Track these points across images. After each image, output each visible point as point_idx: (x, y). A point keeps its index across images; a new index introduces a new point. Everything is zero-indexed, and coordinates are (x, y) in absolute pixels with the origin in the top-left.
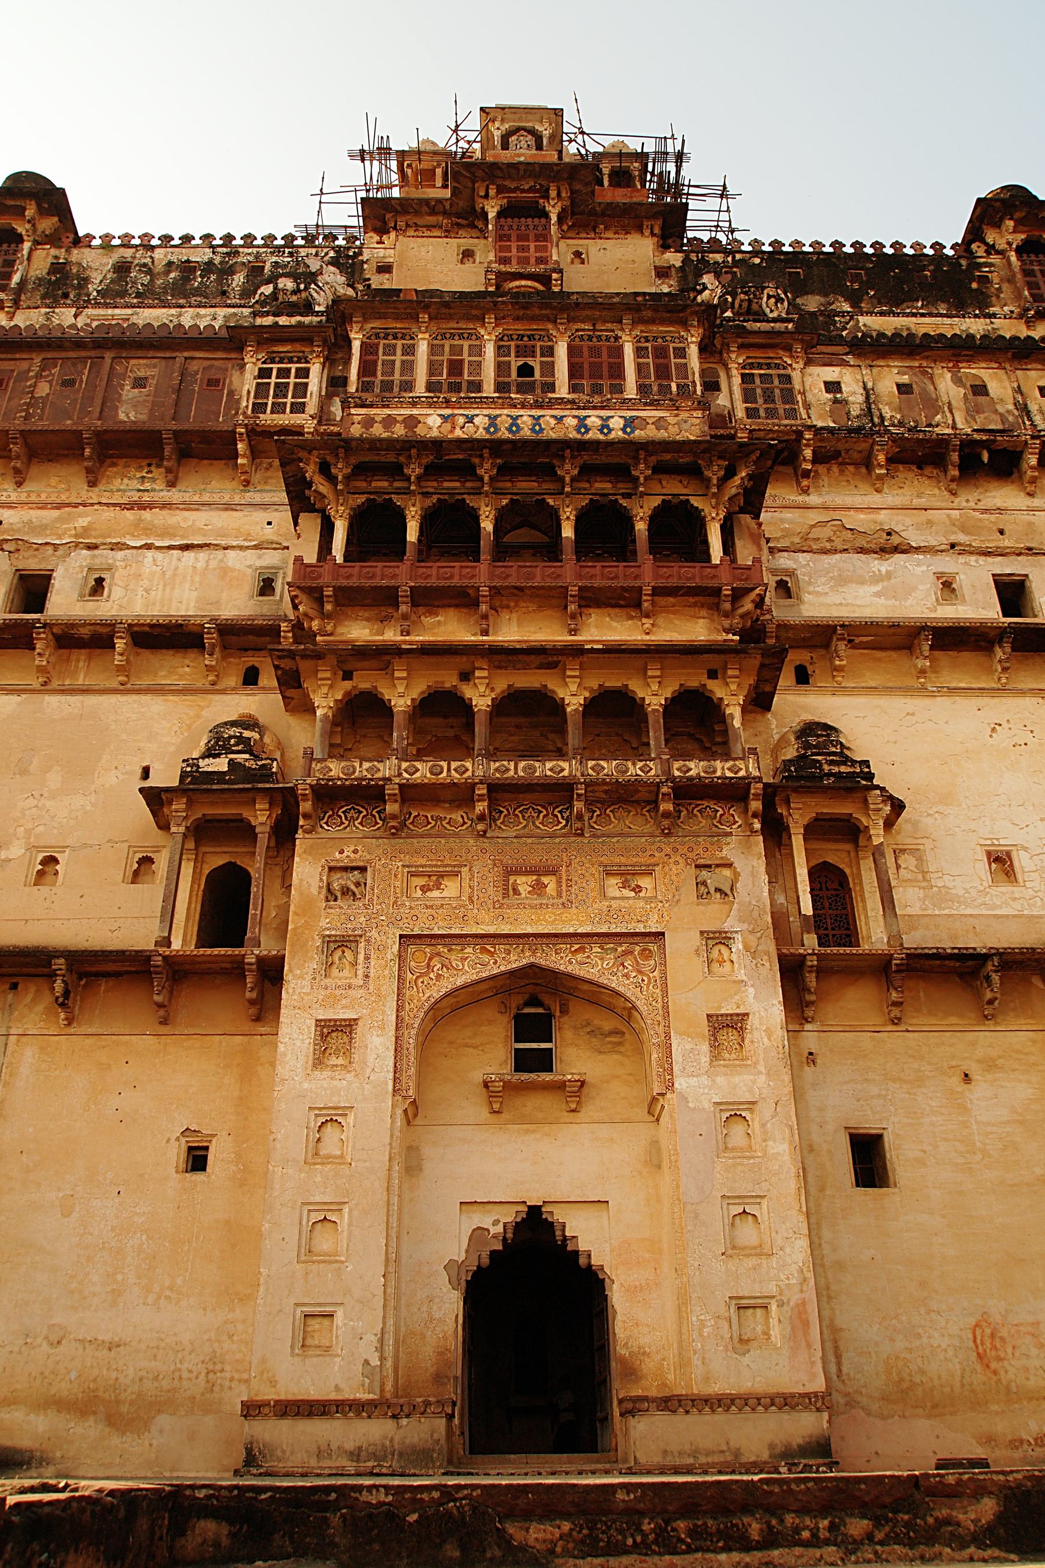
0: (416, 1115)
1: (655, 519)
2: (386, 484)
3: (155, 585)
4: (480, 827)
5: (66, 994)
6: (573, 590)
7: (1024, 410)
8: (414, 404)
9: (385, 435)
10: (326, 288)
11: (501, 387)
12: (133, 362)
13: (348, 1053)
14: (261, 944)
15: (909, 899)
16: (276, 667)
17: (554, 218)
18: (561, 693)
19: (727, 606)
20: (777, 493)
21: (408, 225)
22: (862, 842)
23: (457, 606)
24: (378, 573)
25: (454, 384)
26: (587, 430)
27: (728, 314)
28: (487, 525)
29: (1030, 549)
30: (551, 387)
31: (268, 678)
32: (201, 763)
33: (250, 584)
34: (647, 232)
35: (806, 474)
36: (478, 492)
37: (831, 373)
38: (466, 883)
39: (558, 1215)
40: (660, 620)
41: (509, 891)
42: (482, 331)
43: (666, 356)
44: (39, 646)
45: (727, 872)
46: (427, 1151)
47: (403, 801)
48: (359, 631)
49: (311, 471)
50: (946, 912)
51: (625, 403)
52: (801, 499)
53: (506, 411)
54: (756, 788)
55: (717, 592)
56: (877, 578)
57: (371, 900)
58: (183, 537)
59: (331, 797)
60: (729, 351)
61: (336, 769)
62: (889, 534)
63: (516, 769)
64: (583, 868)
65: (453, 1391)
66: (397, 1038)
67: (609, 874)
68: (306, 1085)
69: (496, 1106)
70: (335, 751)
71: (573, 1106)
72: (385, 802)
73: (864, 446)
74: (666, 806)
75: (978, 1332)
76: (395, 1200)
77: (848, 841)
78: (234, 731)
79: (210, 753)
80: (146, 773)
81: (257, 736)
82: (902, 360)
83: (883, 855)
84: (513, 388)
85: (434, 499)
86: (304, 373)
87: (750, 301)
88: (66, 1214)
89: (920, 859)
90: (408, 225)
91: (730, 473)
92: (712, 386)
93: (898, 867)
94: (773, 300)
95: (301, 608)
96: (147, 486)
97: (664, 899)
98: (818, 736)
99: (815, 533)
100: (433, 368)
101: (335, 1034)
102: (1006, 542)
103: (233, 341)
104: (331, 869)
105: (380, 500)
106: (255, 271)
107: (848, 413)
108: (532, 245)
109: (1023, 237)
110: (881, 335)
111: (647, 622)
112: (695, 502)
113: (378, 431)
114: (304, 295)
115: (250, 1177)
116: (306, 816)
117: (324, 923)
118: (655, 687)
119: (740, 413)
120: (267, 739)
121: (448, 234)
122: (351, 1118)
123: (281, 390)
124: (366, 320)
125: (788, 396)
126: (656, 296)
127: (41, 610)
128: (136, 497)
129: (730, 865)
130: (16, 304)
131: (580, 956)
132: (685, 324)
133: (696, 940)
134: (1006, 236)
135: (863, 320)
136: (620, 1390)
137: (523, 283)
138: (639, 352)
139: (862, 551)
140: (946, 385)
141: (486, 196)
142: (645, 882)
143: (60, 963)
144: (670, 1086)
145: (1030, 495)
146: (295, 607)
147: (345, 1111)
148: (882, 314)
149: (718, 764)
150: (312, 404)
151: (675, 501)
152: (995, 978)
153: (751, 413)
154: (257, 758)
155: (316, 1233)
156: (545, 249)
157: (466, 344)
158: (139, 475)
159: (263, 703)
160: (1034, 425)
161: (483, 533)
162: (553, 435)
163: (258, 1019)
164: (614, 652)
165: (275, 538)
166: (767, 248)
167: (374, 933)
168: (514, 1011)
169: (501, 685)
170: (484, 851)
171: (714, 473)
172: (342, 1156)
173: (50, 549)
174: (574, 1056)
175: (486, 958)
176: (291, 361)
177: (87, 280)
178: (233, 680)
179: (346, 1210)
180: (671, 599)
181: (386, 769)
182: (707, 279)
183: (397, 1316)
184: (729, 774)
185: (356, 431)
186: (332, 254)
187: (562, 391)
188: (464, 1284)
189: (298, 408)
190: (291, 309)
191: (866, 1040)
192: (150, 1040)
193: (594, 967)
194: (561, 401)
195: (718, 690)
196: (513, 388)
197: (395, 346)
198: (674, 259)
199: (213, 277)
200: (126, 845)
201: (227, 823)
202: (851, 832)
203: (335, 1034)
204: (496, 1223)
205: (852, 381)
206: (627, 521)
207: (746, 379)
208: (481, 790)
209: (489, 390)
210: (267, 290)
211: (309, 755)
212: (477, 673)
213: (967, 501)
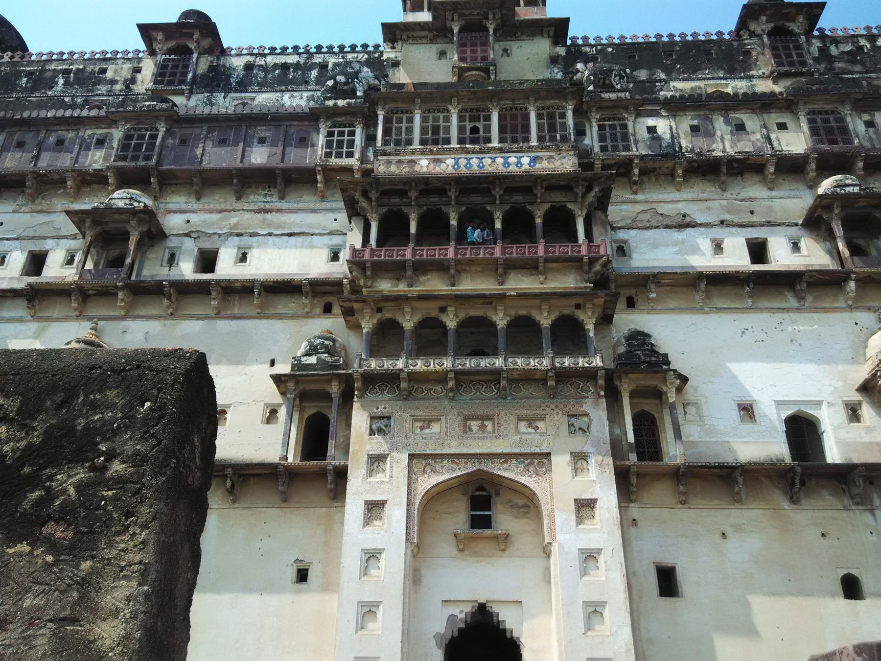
0: (418, 552)
1: (547, 217)
2: (398, 200)
3: (272, 261)
4: (451, 394)
5: (233, 486)
8: (413, 152)
9: (397, 172)
10: (363, 80)
12: (258, 128)
14: (333, 459)
15: (691, 431)
16: (341, 307)
17: (491, 31)
18: (494, 318)
19: (586, 268)
20: (619, 193)
23: (438, 270)
25: (435, 139)
26: (509, 165)
28: (454, 222)
29: (769, 222)
30: (488, 140)
32: (303, 359)
33: (325, 254)
34: (546, 35)
35: (635, 183)
36: (448, 204)
37: (651, 122)
38: (443, 426)
39: (495, 608)
40: (549, 276)
41: (467, 429)
42: (450, 108)
44: (214, 294)
45: (586, 419)
46: (424, 572)
47: (410, 381)
48: (385, 286)
49: (358, 196)
50: (713, 439)
51: (530, 149)
52: (632, 197)
53: (464, 156)
55: (580, 260)
56: (677, 243)
57: (393, 435)
58: (289, 229)
60: (591, 112)
61: (374, 364)
62: (684, 216)
63: (470, 363)
64: (507, 419)
66: (407, 510)
67: (520, 419)
68: (360, 537)
71: (503, 547)
73: (670, 164)
74: (551, 383)
76: (407, 600)
77: (656, 398)
78: (318, 341)
79: (308, 354)
81: (331, 344)
82: (694, 111)
83: (675, 408)
84: (468, 141)
85: (425, 208)
86: (352, 133)
87: (604, 79)
90: (408, 37)
91: (589, 189)
92: (580, 132)
93: (685, 413)
94: (617, 78)
95: (354, 273)
96: (268, 199)
97: (550, 433)
98: (638, 340)
100: (423, 131)
101: (374, 508)
102: (755, 219)
105: (395, 209)
106: (323, 66)
107: (660, 146)
108: (479, 49)
109: (772, 25)
111: (542, 278)
112: (570, 206)
114: (351, 85)
117: (368, 447)
118: (546, 314)
119: (597, 149)
120: (337, 345)
121: (432, 41)
122: (383, 555)
123: (340, 144)
124: (385, 104)
125: (625, 137)
126: (549, 81)
128: (262, 205)
129: (587, 415)
130: (191, 92)
131: (505, 466)
132: (565, 99)
134: (762, 26)
137: (474, 73)
138: (539, 116)
139: (667, 227)
141: (453, 20)
142: (540, 424)
143: (229, 471)
145: (771, 189)
146: (351, 272)
147: (380, 551)
148: (684, 80)
149: (581, 360)
151: (558, 205)
153: (603, 149)
154: (331, 355)
155: (366, 618)
156: (486, 51)
157: (441, 115)
158: (263, 193)
159: (334, 324)
160: (773, 148)
161: (452, 227)
164: (523, 296)
165: (339, 228)
166: (617, 41)
168: (470, 494)
169: (462, 315)
170: (453, 407)
171: (580, 191)
173: (216, 237)
174: (504, 520)
175: (454, 466)
177: (230, 76)
178: (319, 310)
180: (555, 265)
181: (400, 364)
182: (580, 66)
184: (587, 365)
186: (366, 56)
188: (444, 646)
191: (665, 512)
192: (278, 511)
193: (512, 473)
194: (494, 149)
195: (581, 315)
196: (468, 141)
197: (402, 118)
198: (561, 51)
199: (300, 73)
200: (262, 404)
202: (659, 395)
204: (461, 612)
205: (663, 126)
206: (531, 218)
207: (601, 128)
208: (451, 375)
210: (330, 83)
212: (449, 309)
213: (732, 194)
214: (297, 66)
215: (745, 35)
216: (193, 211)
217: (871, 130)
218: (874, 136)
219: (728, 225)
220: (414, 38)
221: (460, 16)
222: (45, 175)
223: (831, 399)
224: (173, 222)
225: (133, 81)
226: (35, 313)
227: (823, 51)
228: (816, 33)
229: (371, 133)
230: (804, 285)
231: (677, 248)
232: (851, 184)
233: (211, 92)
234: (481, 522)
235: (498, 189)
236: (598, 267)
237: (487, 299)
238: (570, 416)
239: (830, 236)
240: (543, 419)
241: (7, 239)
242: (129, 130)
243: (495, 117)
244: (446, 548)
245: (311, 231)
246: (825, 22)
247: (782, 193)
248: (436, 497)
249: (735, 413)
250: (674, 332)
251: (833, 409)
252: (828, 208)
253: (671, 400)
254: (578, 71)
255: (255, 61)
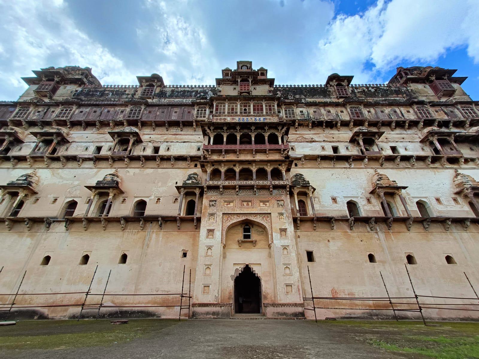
3: (178, 150)
4: (237, 193)
5: (161, 224)
6: (254, 150)
7: (337, 115)
8: (225, 116)
11: (241, 113)
13: (213, 235)
14: (197, 214)
15: (316, 206)
16: (200, 164)
17: (250, 82)
19: (282, 152)
20: (292, 131)
21: (224, 84)
22: (308, 196)
24: (219, 147)
25: (232, 112)
27: (282, 99)
28: (238, 138)
30: (250, 113)
31: (199, 166)
32: (187, 181)
33: (196, 149)
34: (267, 84)
35: (296, 128)
36: (237, 132)
37: (301, 109)
38: (234, 204)
39: (251, 266)
40: (270, 155)
43: (271, 107)
44: (157, 160)
45: (283, 202)
46: (227, 254)
47: (223, 189)
48: (215, 157)
49: (206, 128)
51: (263, 116)
54: (288, 186)
55: (280, 150)
59: (210, 188)
61: (211, 183)
63: (244, 183)
64: (256, 201)
65: (232, 301)
67: (261, 202)
68: (205, 241)
69: (240, 245)
70: (211, 179)
72: (220, 189)
73: (308, 123)
75: (333, 291)
76: (221, 264)
80: (177, 183)
84: (243, 113)
86: (205, 110)
87: (286, 96)
88: (160, 266)
89: (319, 199)
90: (224, 84)
92: (279, 112)
93: (315, 200)
96: (177, 131)
99: (298, 139)
100: (229, 109)
101: (211, 231)
102: (334, 140)
103: (193, 105)
104: (210, 201)
106: (197, 91)
107: (304, 116)
108: (246, 87)
110: (310, 102)
111: (268, 156)
112: (276, 133)
113: (219, 121)
114: (205, 96)
115: (195, 259)
116: (206, 191)
117: (209, 211)
118: (269, 167)
119: (284, 117)
121: (231, 85)
122: (213, 248)
123: (201, 113)
124: (216, 101)
125: (293, 114)
127: (158, 153)
128: (175, 133)
129: (283, 200)
130: (153, 98)
131: (255, 217)
133: (277, 215)
134: (334, 83)
135: (307, 99)
136: (264, 301)
138: (266, 106)
139: (307, 142)
140: (323, 111)
141: (238, 78)
142: (267, 204)
143: (160, 219)
144: (273, 242)
145: (339, 131)
146: (204, 153)
147: (212, 246)
148: (310, 98)
149: (281, 182)
150: (207, 116)
152: (334, 222)
153: (286, 117)
154: (197, 180)
155: (206, 270)
157: (234, 105)
159: (198, 170)
161: (238, 139)
162: (250, 121)
163: (196, 229)
166: (289, 86)
167: (218, 213)
169: (241, 167)
171: (280, 128)
172: (211, 255)
173: (160, 142)
174: (254, 236)
175: (238, 217)
176: (203, 108)
177: (166, 94)
178: (193, 166)
179: (212, 266)
180: (272, 151)
182: (278, 92)
183: (221, 287)
184: (283, 184)
185: (215, 121)
187: (252, 113)
189: (204, 117)
190: (203, 98)
191: (309, 233)
193: (258, 219)
194: (252, 115)
195: (280, 168)
196: (243, 113)
201: (191, 192)
202: (305, 194)
203: (211, 231)
204: (240, 268)
205: (304, 110)
206: (264, 137)
207: (286, 110)
208: (237, 187)
209: (239, 113)
210: (199, 95)
211: (206, 180)
212: (237, 165)
214: (188, 91)
215: (328, 85)
216: (152, 134)
217: (370, 113)
218: (371, 115)
219: (326, 142)
220: (226, 84)
221: (241, 77)
222: (102, 122)
223: (361, 196)
224: (144, 138)
225: (135, 94)
226: (96, 166)
227: (353, 91)
228: (350, 86)
229: (211, 110)
230: (351, 160)
231: (310, 148)
232: (365, 129)
233: (160, 98)
234: (247, 237)
235: (253, 127)
236: (286, 152)
237: (250, 162)
238: (277, 201)
239: (358, 144)
240: (268, 202)
241: (89, 142)
242: (132, 108)
243: (252, 106)
244: (236, 246)
245: (191, 141)
246: (353, 82)
247: (342, 132)
248: (232, 227)
249: (331, 201)
250: (311, 174)
251: (362, 199)
252: (358, 136)
253: (310, 196)
254: (278, 94)
255: (175, 89)
